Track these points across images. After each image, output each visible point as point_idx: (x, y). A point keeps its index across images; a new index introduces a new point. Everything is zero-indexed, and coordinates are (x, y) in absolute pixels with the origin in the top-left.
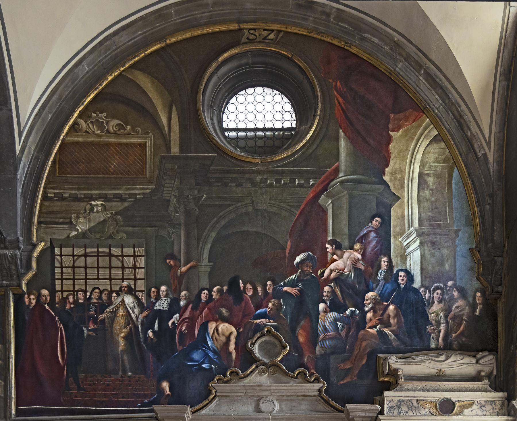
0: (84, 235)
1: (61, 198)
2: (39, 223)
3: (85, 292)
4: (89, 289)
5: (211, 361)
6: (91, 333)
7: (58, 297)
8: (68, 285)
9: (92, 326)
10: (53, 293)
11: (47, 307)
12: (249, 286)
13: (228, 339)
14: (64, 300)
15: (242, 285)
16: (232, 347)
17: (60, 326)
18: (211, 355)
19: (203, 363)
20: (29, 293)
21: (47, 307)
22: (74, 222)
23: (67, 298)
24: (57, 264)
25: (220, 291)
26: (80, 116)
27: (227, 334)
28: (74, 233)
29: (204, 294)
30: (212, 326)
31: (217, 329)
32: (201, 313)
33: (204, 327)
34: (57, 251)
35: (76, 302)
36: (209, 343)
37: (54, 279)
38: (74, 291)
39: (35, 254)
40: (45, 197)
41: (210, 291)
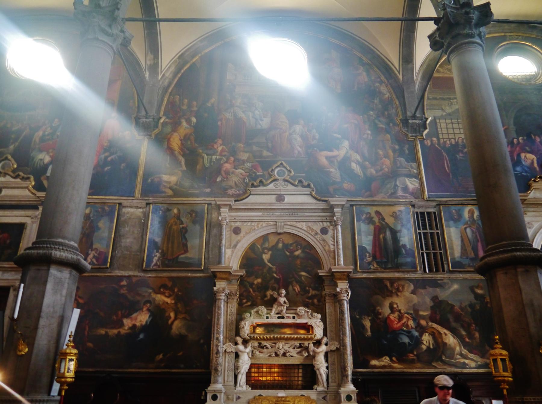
0: (449, 114)
1: (436, 99)
2: (427, 109)
3: (455, 139)
4: (457, 138)
5: (526, 172)
6: (461, 158)
7: (442, 141)
8: (445, 136)
9: (461, 155)
10: (438, 139)
11: (437, 146)
12: (537, 137)
13: (532, 163)
14: (445, 143)
15: (533, 137)
16: (536, 165)
17: (445, 155)
18: (526, 169)
19: (522, 172)
20: (427, 139)
21: (437, 146)
22: (443, 108)
23: (446, 142)
24: (439, 127)
25: (523, 139)
26: (440, 66)
27: (532, 158)
28: (444, 114)
29: (515, 141)
30: (523, 155)
31: (526, 157)
32: (516, 149)
33: (519, 155)
34: (438, 121)
35: (451, 143)
36: (524, 163)
37: (438, 133)
38: (449, 138)
39: (428, 122)
40: (428, 99)
41: (518, 139)
